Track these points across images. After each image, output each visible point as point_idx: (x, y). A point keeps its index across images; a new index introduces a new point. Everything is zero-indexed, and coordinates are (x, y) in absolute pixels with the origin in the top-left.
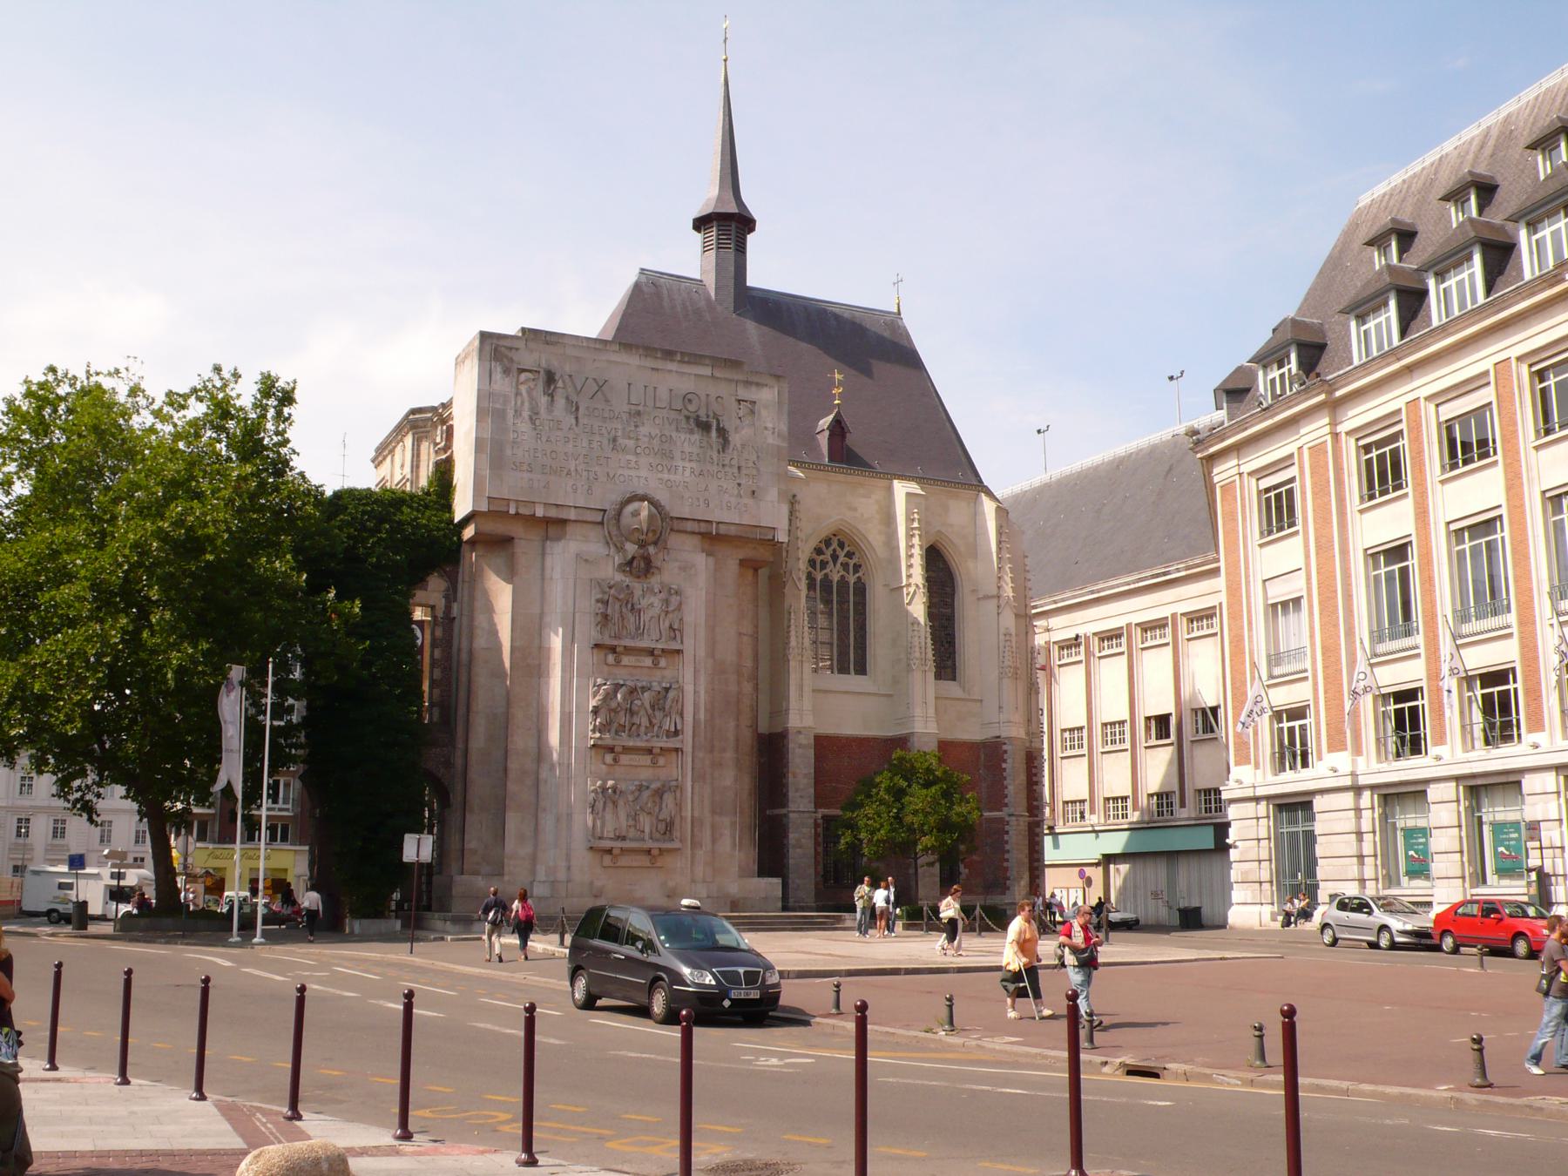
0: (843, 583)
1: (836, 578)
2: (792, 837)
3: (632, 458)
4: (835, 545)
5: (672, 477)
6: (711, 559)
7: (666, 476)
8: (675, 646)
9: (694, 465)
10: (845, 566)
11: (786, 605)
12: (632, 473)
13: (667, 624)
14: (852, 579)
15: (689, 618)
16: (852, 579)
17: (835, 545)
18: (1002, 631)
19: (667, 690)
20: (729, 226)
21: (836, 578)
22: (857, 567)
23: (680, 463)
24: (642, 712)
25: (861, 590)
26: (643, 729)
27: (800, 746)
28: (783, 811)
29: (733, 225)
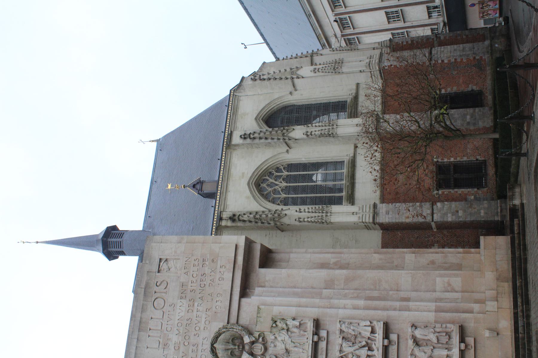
0: (287, 179)
1: (284, 184)
2: (450, 218)
3: (191, 347)
4: (264, 185)
5: (203, 320)
6: (258, 290)
7: (202, 325)
8: (310, 326)
9: (196, 304)
10: (277, 178)
11: (297, 223)
12: (200, 348)
13: (295, 330)
14: (285, 173)
15: (293, 311)
16: (285, 173)
17: (264, 185)
18: (313, 74)
19: (341, 331)
20: (111, 243)
21: (284, 184)
22: (278, 170)
23: (195, 313)
24: (357, 352)
25: (291, 167)
26: (370, 353)
27: (387, 213)
28: (433, 224)
29: (109, 240)
